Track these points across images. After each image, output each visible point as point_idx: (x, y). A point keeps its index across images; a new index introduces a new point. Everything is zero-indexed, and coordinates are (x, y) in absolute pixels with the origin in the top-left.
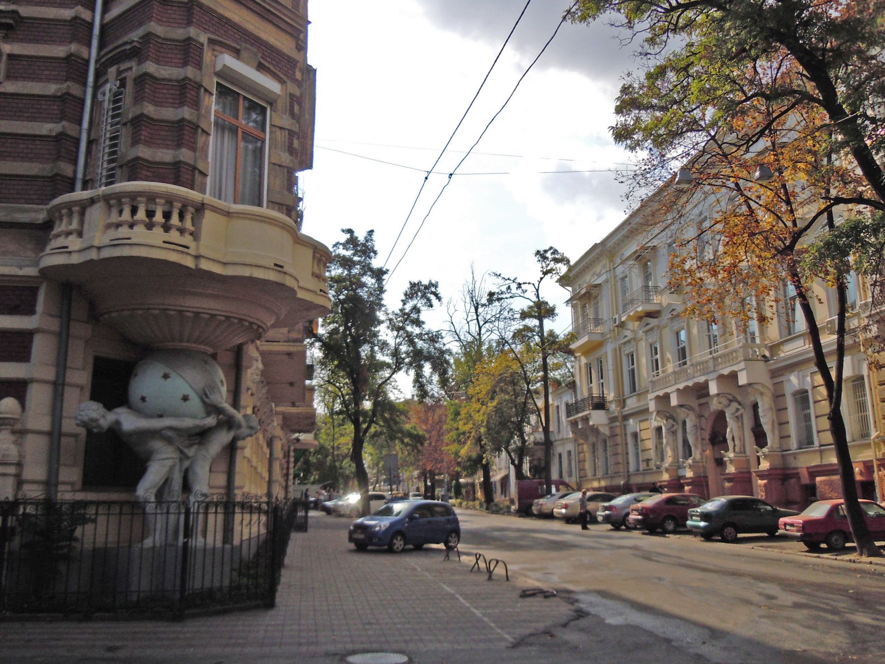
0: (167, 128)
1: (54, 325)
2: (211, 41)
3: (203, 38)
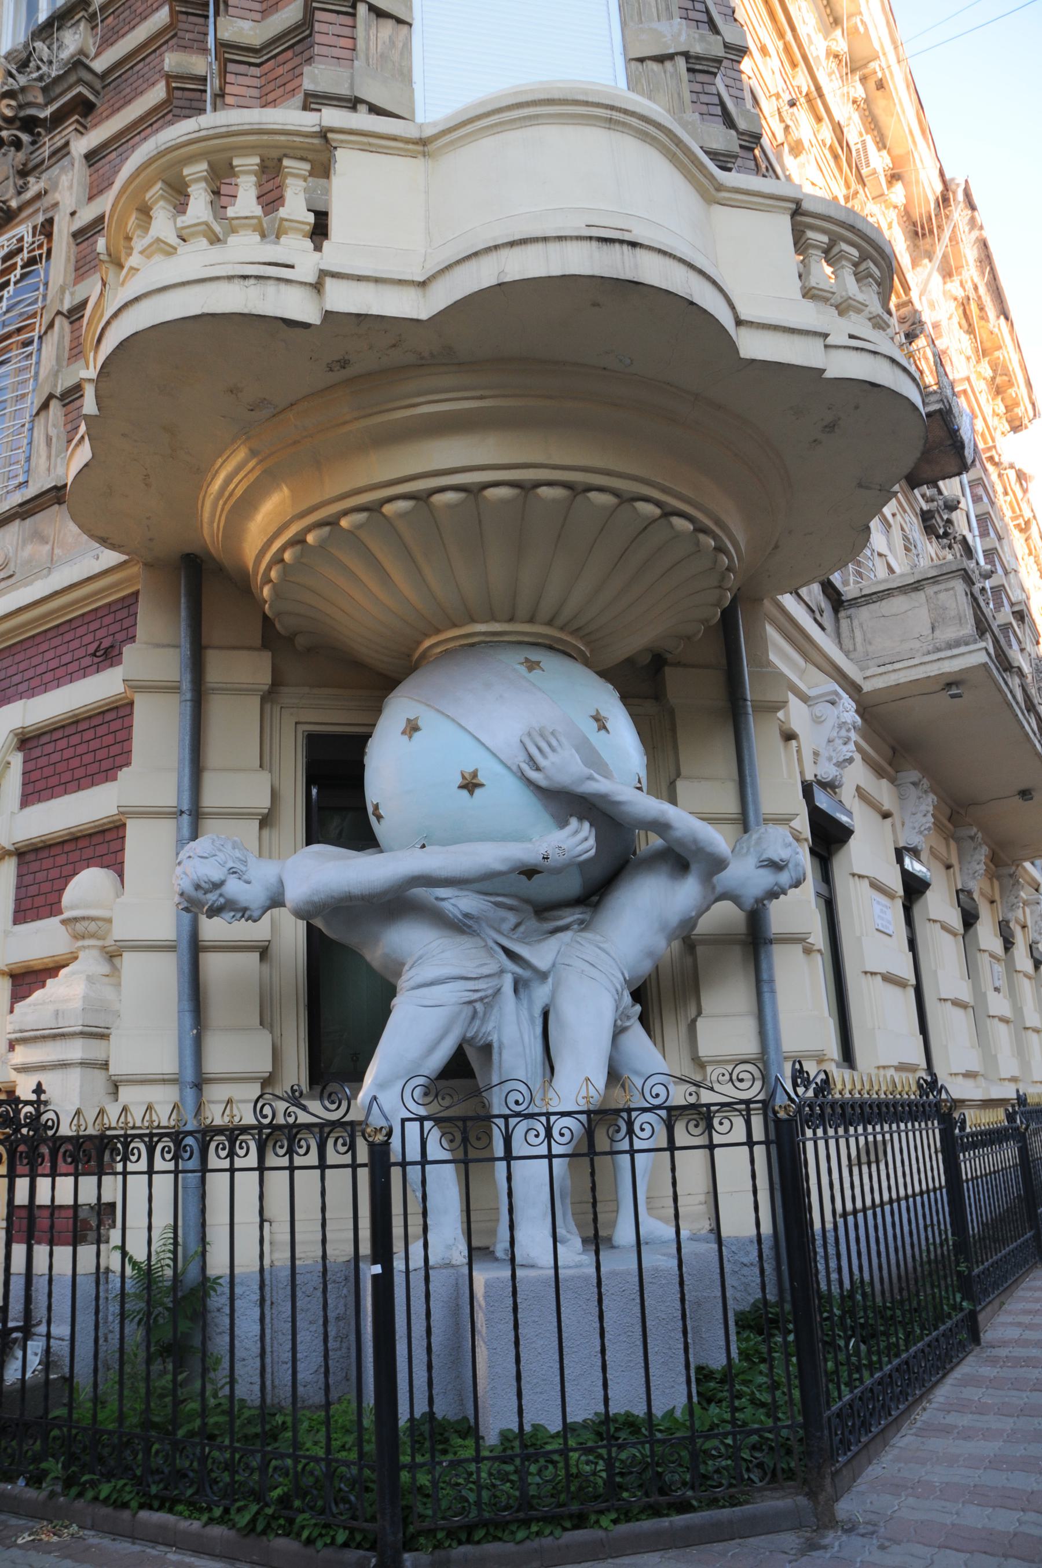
0: (289, 54)
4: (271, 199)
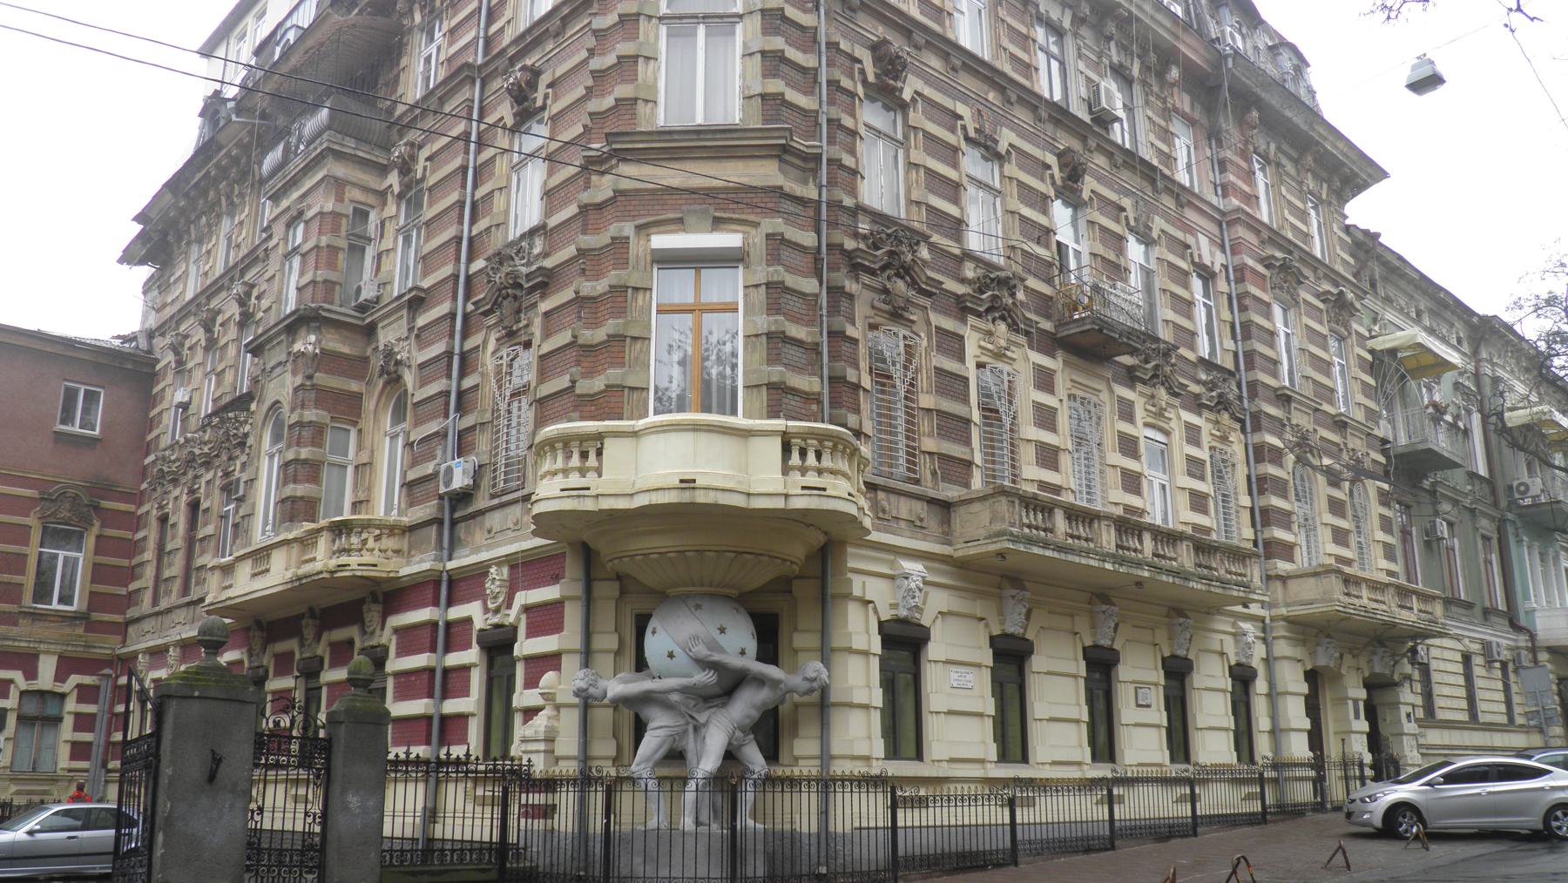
1: (577, 589)
2: (639, 228)
3: (628, 229)
4: (584, 455)
